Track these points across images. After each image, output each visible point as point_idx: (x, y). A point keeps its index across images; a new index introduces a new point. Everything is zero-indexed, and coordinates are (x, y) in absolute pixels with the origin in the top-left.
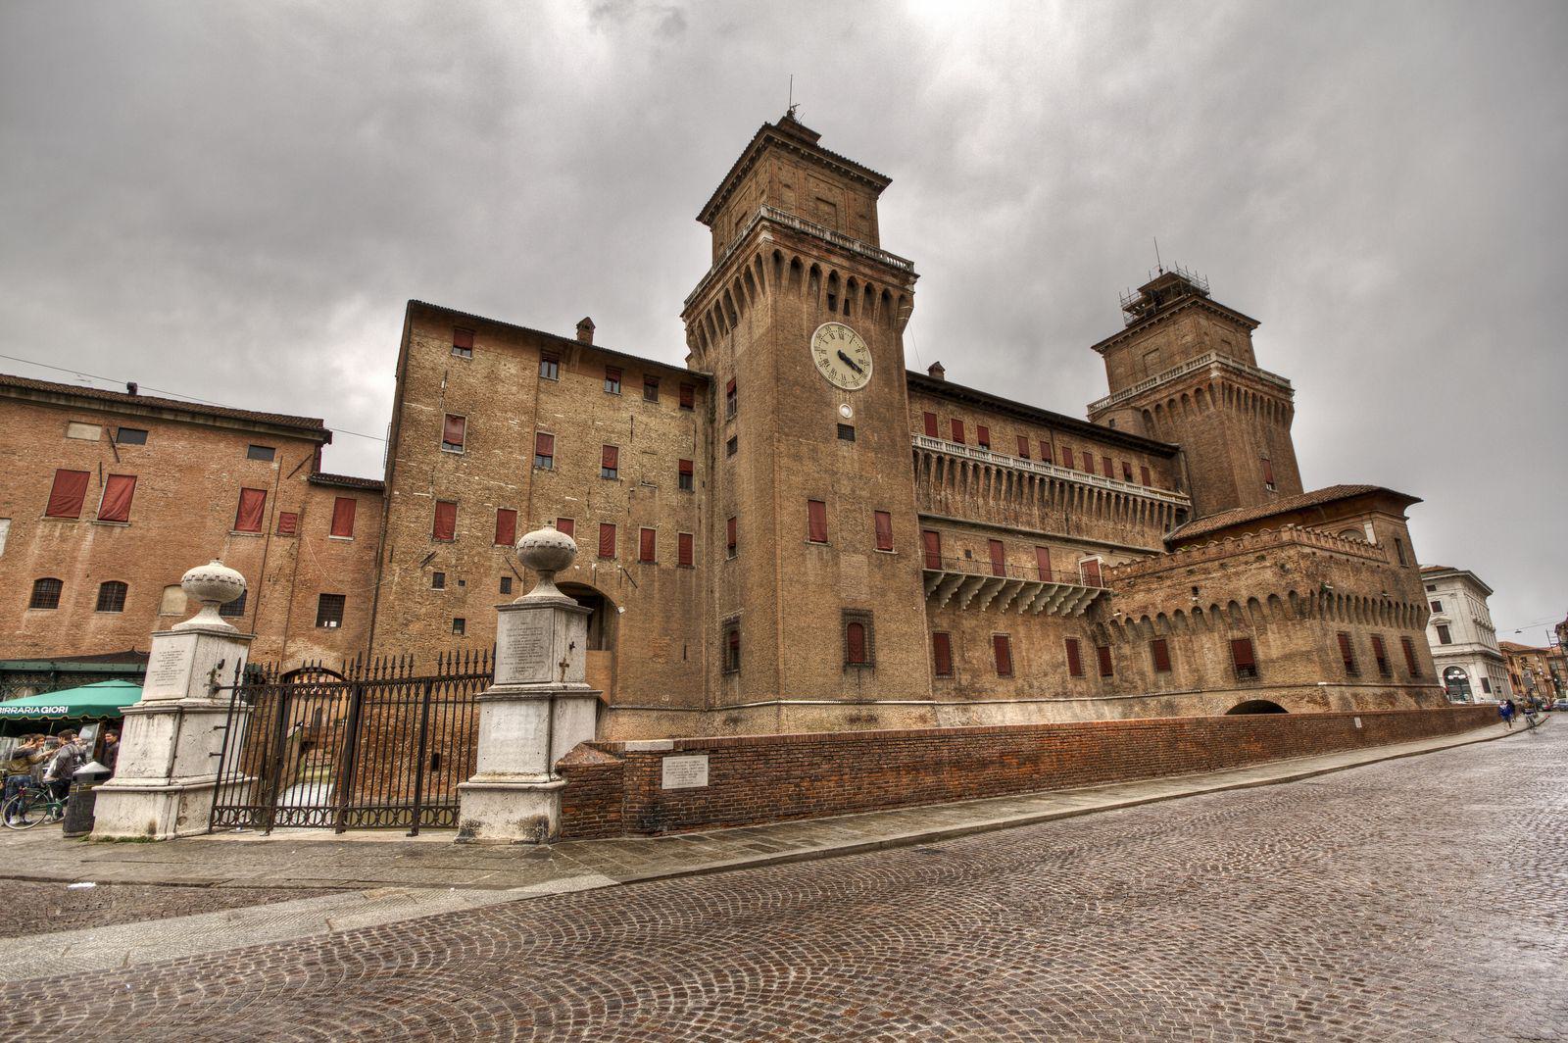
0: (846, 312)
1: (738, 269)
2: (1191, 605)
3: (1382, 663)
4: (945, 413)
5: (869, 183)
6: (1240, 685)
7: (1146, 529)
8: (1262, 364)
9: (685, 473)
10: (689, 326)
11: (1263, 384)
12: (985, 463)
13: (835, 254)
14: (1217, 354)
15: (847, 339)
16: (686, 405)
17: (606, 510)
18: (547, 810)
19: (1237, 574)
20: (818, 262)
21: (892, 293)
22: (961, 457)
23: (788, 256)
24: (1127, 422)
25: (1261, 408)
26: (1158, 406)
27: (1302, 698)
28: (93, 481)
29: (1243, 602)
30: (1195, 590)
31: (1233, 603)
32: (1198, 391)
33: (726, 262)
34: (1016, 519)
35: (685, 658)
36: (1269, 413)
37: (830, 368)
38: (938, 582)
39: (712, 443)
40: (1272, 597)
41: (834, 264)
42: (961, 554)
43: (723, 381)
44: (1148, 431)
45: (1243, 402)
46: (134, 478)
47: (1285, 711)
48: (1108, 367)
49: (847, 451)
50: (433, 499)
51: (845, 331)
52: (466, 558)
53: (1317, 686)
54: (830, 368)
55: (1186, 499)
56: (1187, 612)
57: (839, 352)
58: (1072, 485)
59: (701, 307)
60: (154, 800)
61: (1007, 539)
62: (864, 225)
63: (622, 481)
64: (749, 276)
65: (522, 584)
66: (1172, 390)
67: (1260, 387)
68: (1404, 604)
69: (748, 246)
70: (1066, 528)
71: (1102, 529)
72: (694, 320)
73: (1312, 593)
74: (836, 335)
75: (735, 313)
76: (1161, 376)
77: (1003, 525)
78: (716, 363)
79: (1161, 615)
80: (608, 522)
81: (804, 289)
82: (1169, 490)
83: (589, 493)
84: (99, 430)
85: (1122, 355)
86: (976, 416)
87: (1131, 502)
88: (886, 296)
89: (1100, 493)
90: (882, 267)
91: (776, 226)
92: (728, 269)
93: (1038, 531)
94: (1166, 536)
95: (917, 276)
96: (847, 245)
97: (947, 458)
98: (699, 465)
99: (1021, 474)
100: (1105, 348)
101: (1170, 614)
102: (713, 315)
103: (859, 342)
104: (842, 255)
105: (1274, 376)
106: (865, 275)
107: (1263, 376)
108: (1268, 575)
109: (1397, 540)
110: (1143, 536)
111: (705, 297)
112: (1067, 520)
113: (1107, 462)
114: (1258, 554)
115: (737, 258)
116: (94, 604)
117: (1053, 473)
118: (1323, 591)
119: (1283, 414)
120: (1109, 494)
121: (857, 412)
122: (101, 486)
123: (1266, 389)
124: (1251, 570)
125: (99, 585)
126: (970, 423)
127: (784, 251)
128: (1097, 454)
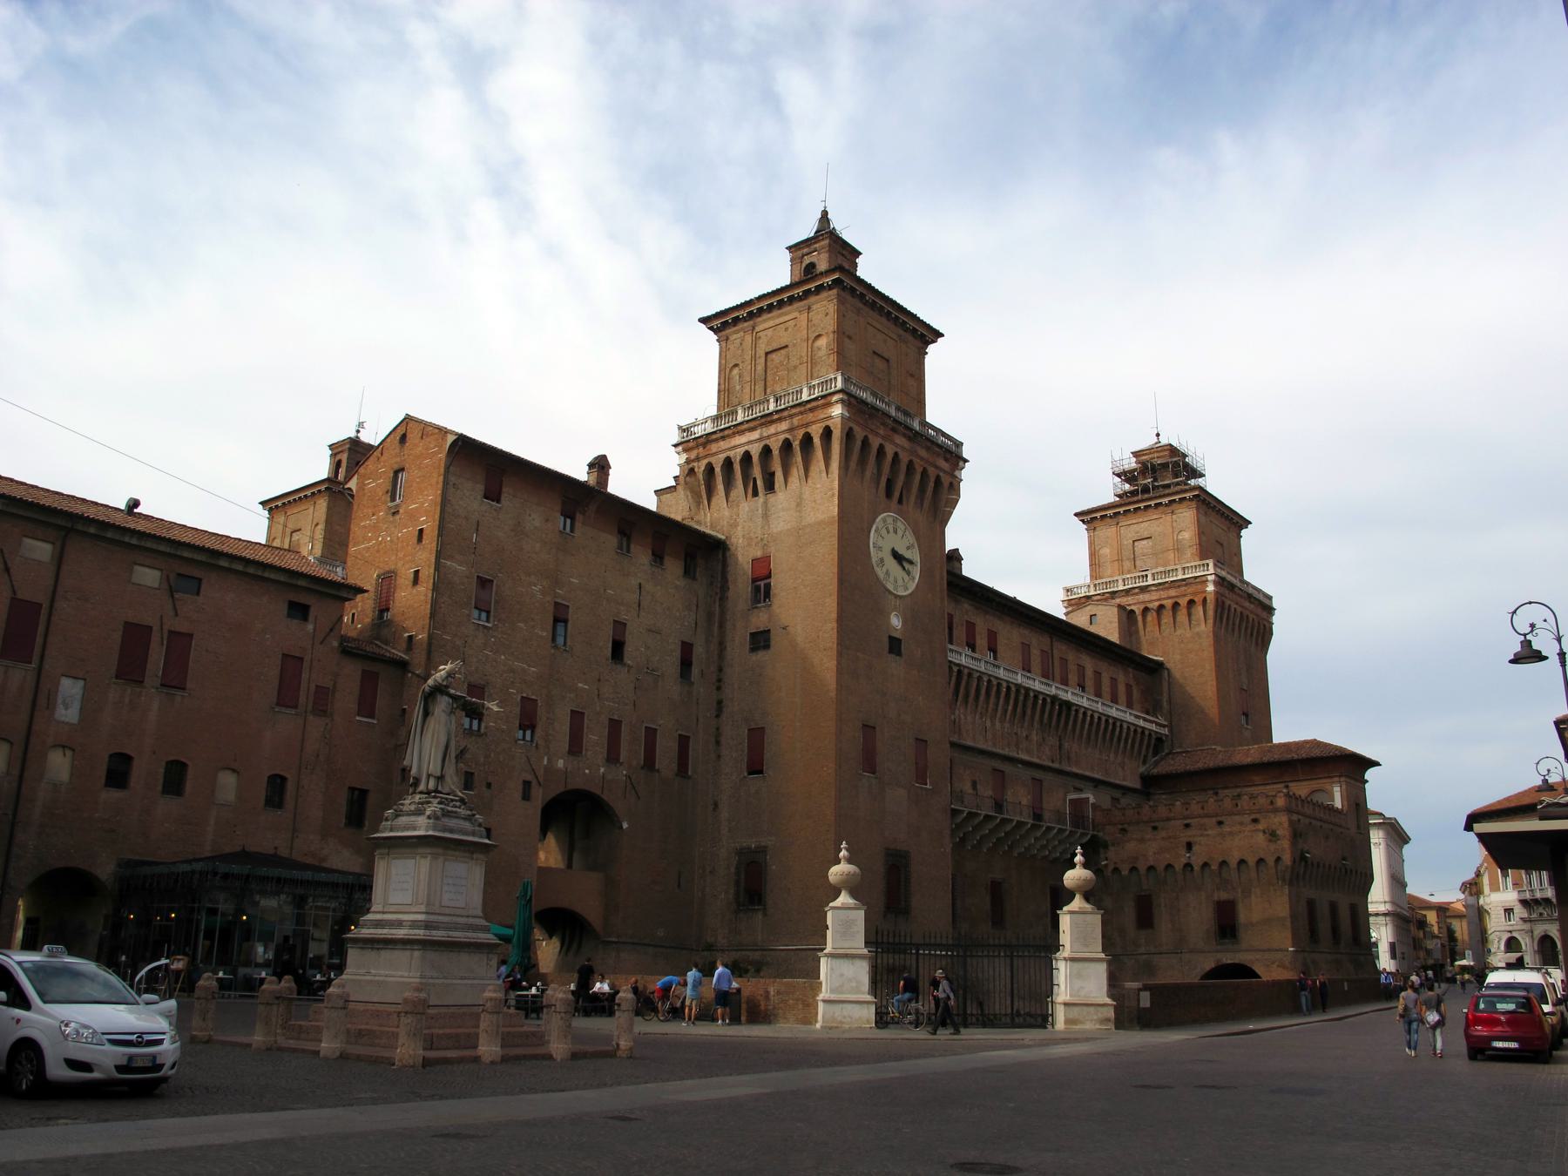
0: (900, 501)
1: (791, 430)
2: (1184, 861)
3: (1335, 931)
4: (966, 611)
5: (923, 336)
6: (1219, 947)
7: (1126, 760)
8: (1246, 578)
9: (686, 663)
10: (688, 461)
11: (1250, 602)
12: (997, 678)
14: (1215, 565)
15: (900, 533)
16: (688, 572)
17: (613, 702)
18: (1111, 1013)
19: (1231, 833)
20: (883, 442)
21: (943, 480)
22: (977, 671)
23: (859, 433)
24: (1111, 622)
25: (1246, 628)
26: (1146, 610)
27: (1273, 963)
28: (155, 637)
29: (1233, 863)
30: (1189, 846)
31: (1224, 863)
32: (1191, 603)
34: (1017, 746)
35: (679, 886)
36: (1252, 635)
37: (884, 569)
38: (959, 819)
39: (722, 626)
40: (1261, 861)
41: (897, 445)
42: (968, 787)
43: (744, 554)
44: (1131, 635)
45: (1231, 622)
46: (191, 636)
47: (1258, 976)
48: (1091, 544)
49: (895, 666)
50: (464, 682)
51: (899, 524)
52: (492, 755)
53: (1288, 951)
54: (884, 569)
55: (1164, 726)
56: (1178, 867)
57: (893, 550)
58: (1068, 704)
59: (714, 447)
60: (868, 1009)
61: (1007, 768)
62: (911, 382)
63: (629, 666)
64: (807, 440)
65: (541, 790)
66: (1164, 594)
67: (1247, 604)
68: (1356, 872)
69: (811, 410)
70: (1058, 757)
71: (1089, 761)
72: (698, 459)
73: (1294, 862)
74: (891, 530)
75: (773, 474)
76: (1153, 574)
77: (1006, 752)
78: (735, 525)
79: (1151, 868)
80: (616, 717)
82: (1148, 713)
83: (599, 680)
84: (157, 574)
85: (1107, 532)
86: (987, 617)
87: (1118, 729)
88: (938, 481)
89: (1092, 716)
90: (937, 449)
91: (852, 400)
92: (772, 422)
93: (1035, 760)
94: (1142, 769)
95: (966, 461)
97: (966, 671)
98: (699, 651)
99: (1027, 690)
100: (1089, 518)
101: (1161, 867)
102: (737, 467)
103: (910, 538)
104: (904, 435)
105: (1259, 590)
106: (922, 459)
107: (1251, 591)
108: (1261, 838)
109: (1357, 805)
110: (1123, 768)
111: (723, 438)
112: (1060, 747)
113: (1098, 674)
114: (1253, 816)
115: (791, 416)
116: (160, 788)
117: (1053, 691)
118: (1303, 858)
119: (1263, 639)
120: (1099, 718)
121: (904, 623)
122: (162, 644)
123: (1252, 606)
124: (1244, 831)
125: (164, 764)
126: (982, 623)
128: (1089, 663)
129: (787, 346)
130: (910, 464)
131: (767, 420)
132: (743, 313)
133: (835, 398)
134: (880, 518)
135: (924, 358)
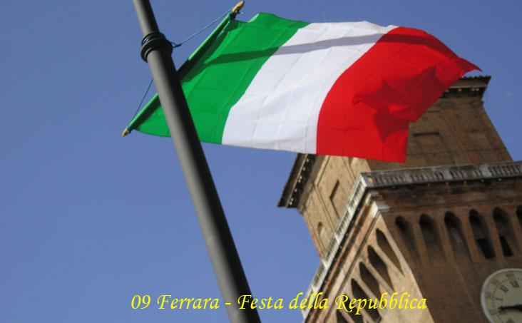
0: (507, 252)
13: (465, 192)
23: (412, 217)
33: (339, 250)
41: (468, 204)
62: (480, 137)
69: (361, 223)
81: (447, 247)
91: (385, 191)
96: (474, 175)
104: (474, 190)
106: (510, 200)
115: (352, 241)
127: (406, 215)
129: (337, 184)
130: (499, 216)
131: (340, 257)
132: (299, 177)
133: (367, 200)
134: (486, 282)
135: (483, 109)
